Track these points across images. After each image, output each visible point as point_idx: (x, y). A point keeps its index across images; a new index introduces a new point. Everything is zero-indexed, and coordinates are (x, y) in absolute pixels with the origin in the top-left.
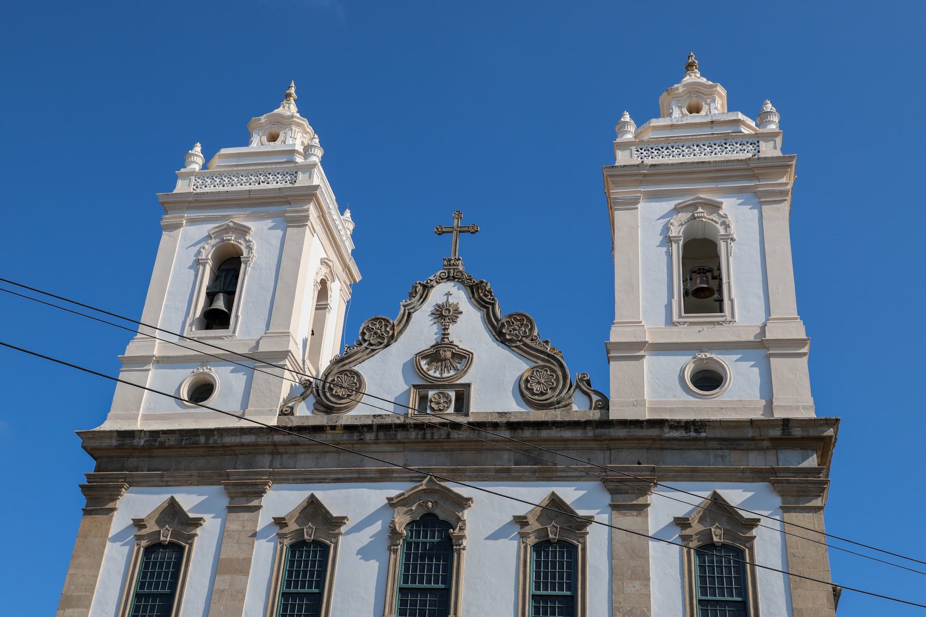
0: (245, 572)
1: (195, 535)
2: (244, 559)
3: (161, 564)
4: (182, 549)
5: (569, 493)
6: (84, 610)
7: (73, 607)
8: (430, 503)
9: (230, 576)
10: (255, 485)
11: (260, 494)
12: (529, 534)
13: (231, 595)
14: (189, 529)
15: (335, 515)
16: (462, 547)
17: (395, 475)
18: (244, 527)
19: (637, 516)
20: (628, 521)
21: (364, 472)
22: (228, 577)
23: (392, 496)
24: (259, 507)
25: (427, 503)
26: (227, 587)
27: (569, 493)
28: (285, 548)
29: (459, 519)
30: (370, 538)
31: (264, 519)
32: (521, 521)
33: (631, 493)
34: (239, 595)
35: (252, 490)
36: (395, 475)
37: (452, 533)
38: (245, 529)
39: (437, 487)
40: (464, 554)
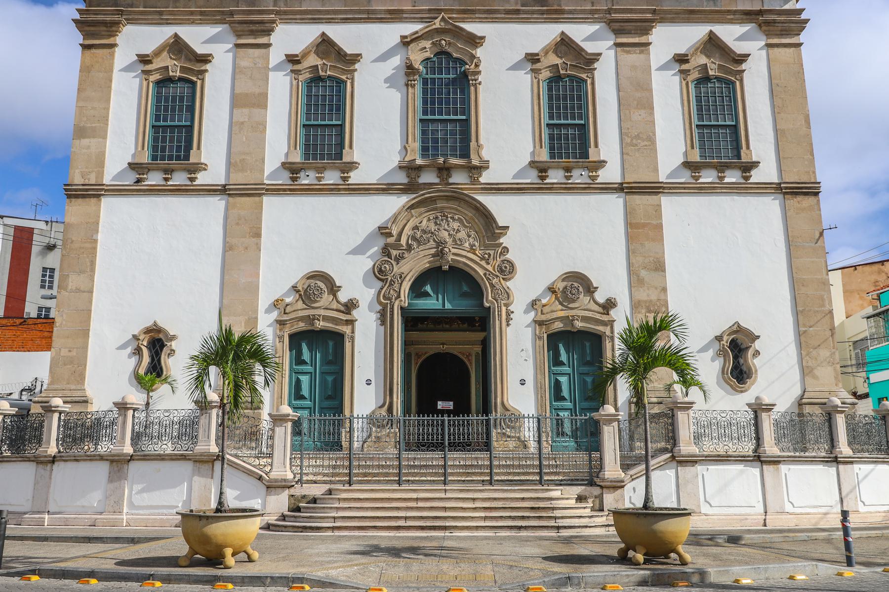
0: (265, 107)
1: (206, 71)
2: (260, 94)
3: (174, 98)
4: (194, 83)
5: (579, 32)
6: (101, 140)
7: (89, 137)
8: (443, 42)
9: (248, 110)
10: (262, 22)
11: (268, 32)
12: (540, 70)
13: (252, 127)
14: (198, 65)
15: (349, 52)
16: (477, 82)
17: (405, 16)
18: (255, 64)
19: (640, 53)
20: (633, 58)
21: (374, 12)
22: (246, 111)
23: (407, 33)
24: (268, 46)
25: (440, 40)
26: (247, 120)
27: (579, 32)
28: (300, 83)
29: (473, 57)
30: (393, 70)
31: (276, 56)
32: (532, 59)
33: (634, 34)
34: (260, 127)
35: (260, 28)
36: (405, 16)
37: (468, 69)
38: (257, 65)
39: (450, 27)
40: (481, 88)
